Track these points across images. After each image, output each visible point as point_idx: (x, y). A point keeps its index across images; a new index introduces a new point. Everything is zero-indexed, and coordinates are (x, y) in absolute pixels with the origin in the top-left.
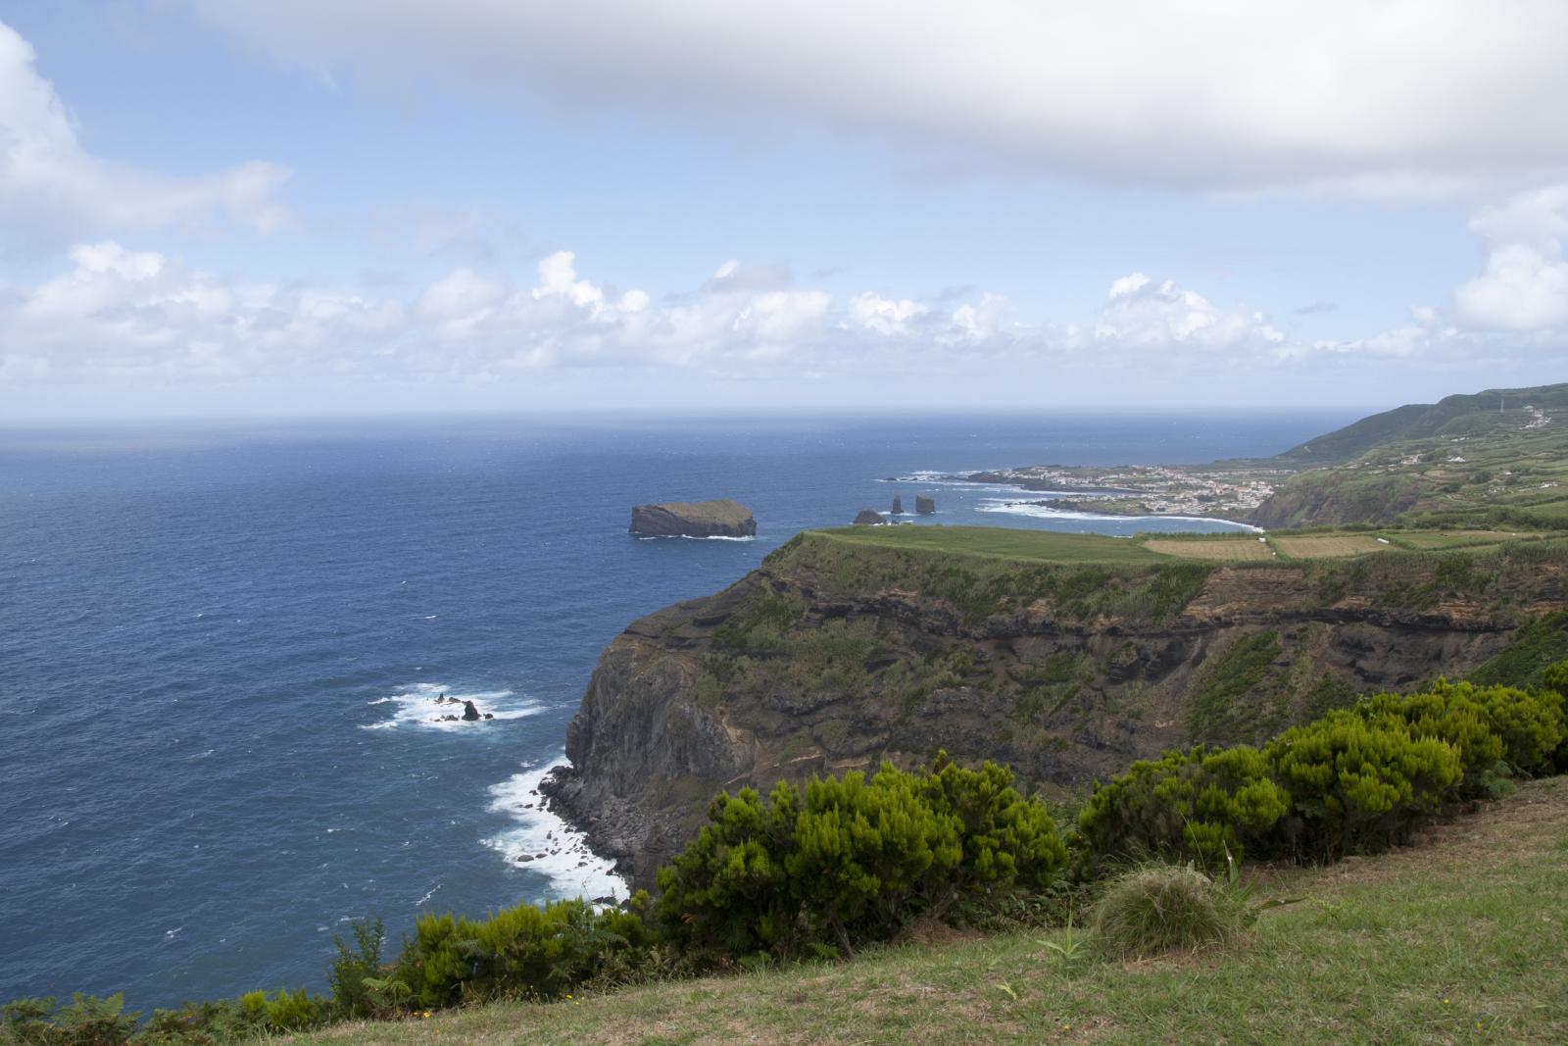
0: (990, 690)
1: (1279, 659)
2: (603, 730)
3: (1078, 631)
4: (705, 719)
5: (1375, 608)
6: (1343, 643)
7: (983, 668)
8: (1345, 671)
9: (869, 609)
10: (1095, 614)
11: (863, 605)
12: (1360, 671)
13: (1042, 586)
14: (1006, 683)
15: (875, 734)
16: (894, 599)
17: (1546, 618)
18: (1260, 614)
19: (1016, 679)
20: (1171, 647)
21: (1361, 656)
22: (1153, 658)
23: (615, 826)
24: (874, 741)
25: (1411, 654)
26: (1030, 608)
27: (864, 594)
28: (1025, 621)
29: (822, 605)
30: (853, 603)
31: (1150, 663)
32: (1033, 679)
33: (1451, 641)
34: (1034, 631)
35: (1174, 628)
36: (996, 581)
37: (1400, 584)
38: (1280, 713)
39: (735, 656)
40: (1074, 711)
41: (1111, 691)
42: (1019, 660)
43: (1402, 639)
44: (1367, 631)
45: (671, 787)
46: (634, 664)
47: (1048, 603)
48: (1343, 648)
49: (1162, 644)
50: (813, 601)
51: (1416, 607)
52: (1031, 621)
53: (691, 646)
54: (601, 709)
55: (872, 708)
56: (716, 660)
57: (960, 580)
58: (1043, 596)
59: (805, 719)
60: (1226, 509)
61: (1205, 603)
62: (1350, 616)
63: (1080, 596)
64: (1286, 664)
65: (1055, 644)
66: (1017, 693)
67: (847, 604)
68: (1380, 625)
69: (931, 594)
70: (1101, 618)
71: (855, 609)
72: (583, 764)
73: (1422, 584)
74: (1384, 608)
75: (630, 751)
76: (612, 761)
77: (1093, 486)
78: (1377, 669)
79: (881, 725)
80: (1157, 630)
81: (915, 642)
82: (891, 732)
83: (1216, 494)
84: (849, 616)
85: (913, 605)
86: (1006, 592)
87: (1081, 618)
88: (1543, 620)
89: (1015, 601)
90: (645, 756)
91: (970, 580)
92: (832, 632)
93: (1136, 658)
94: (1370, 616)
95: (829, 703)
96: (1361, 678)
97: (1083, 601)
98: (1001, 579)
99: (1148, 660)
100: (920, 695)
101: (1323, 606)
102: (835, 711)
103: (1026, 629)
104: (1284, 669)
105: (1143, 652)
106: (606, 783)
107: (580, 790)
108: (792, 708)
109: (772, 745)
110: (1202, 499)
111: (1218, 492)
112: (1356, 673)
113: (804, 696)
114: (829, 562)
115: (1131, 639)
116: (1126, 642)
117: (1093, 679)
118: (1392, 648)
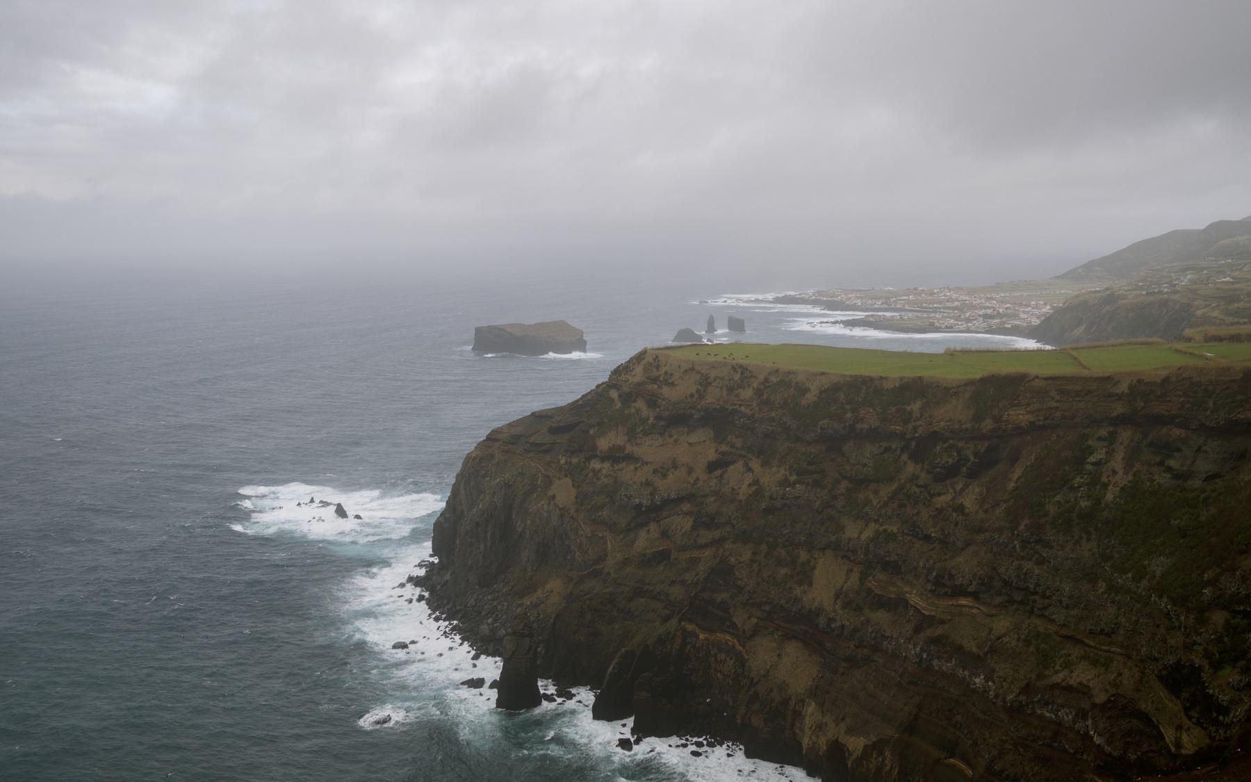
1: (1092, 459)
11: (702, 413)
19: (845, 478)
23: (480, 613)
24: (717, 534)
30: (693, 411)
31: (970, 463)
39: (588, 459)
49: (983, 446)
52: (859, 426)
53: (547, 451)
60: (1009, 326)
65: (880, 446)
71: (695, 417)
77: (886, 306)
78: (1185, 468)
82: (734, 527)
83: (998, 312)
91: (803, 390)
93: (957, 459)
99: (969, 461)
107: (447, 581)
110: (986, 316)
111: (1001, 310)
112: (1164, 472)
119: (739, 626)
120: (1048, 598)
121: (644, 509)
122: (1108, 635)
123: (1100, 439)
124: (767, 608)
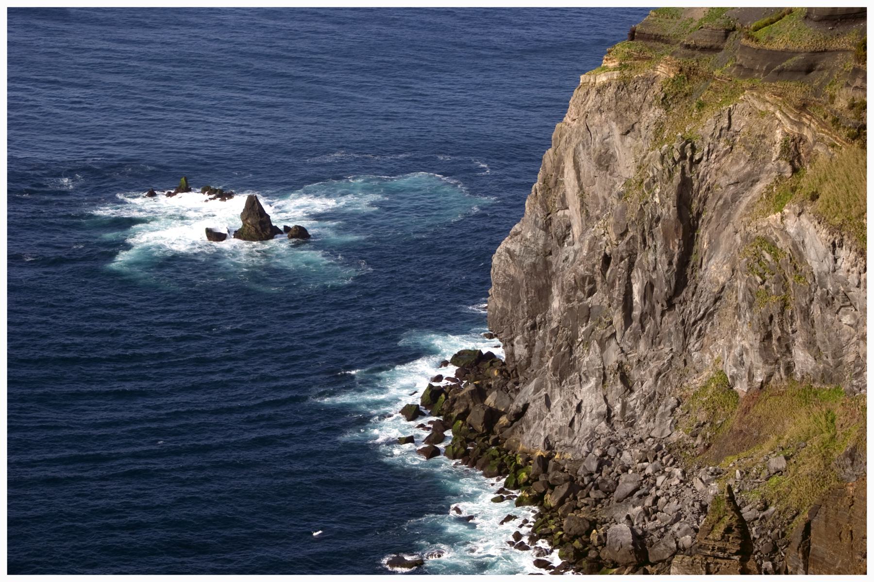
2: (581, 269)
23: (609, 493)
54: (573, 213)
76: (603, 345)
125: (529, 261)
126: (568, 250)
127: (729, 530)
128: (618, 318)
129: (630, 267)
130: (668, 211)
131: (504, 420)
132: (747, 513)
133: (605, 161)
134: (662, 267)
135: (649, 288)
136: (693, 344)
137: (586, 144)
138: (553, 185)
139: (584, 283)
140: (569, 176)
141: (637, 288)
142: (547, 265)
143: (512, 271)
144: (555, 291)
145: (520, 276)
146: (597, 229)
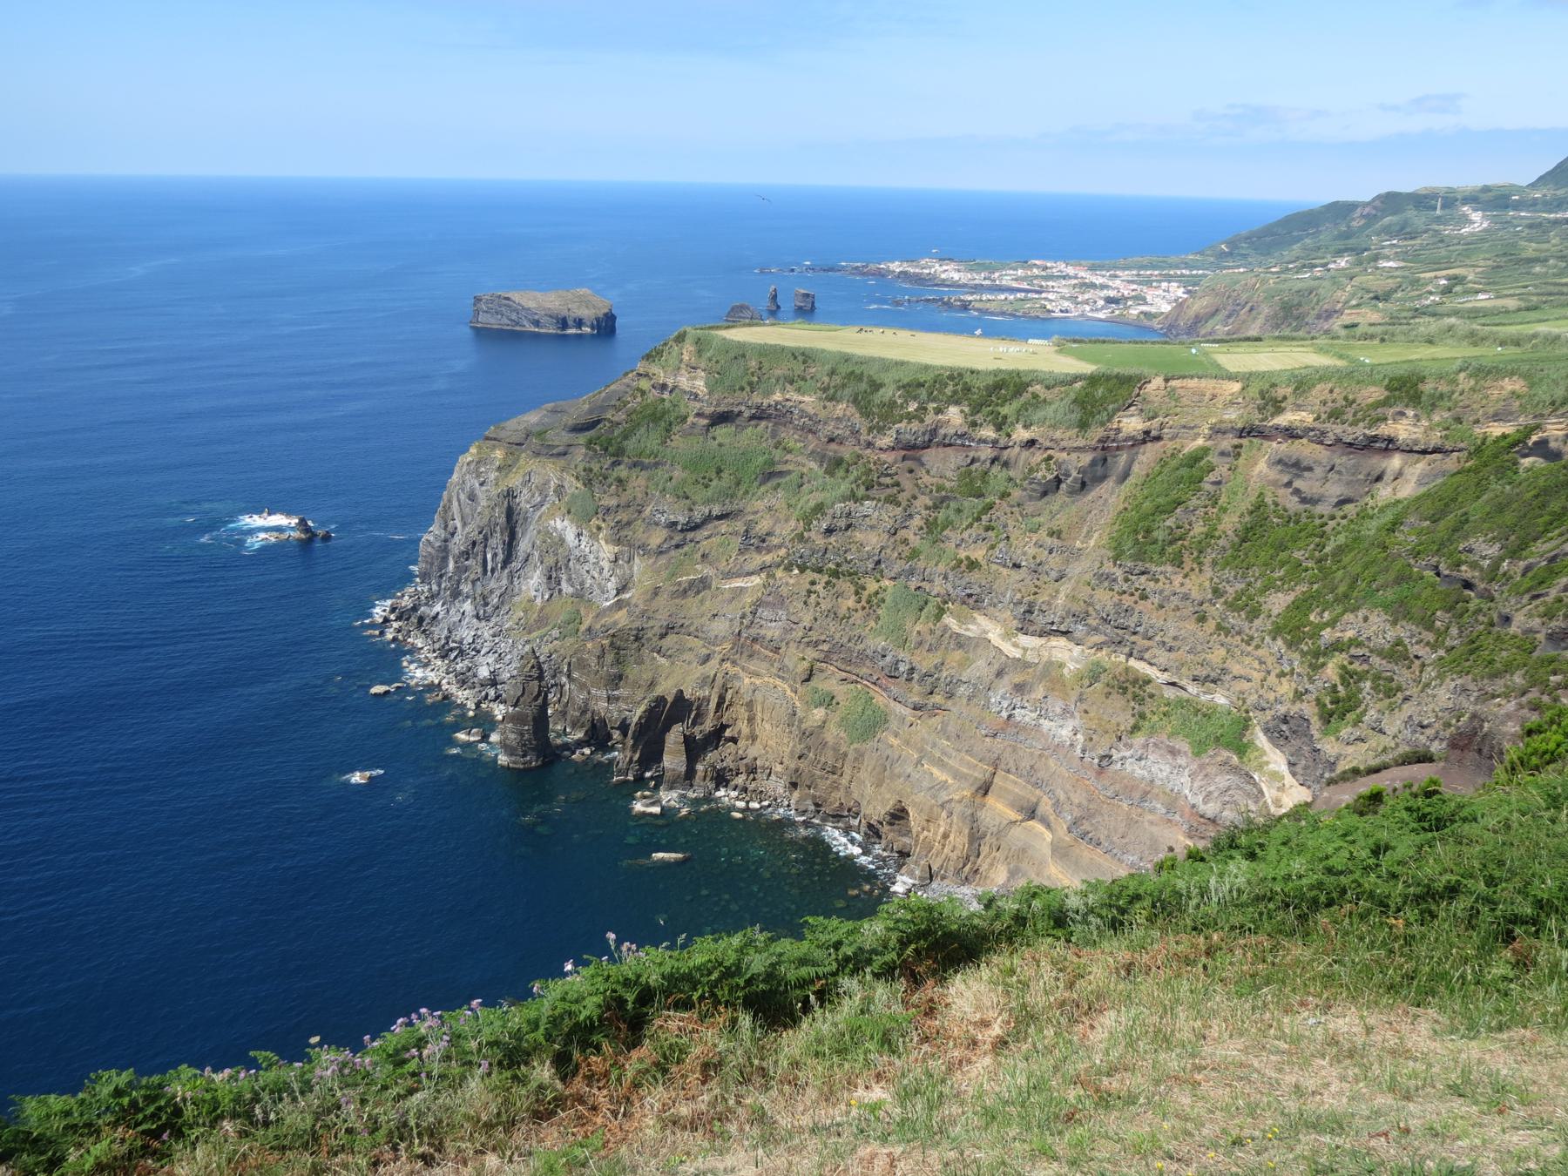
0: (898, 504)
3: (995, 442)
4: (579, 535)
5: (1317, 425)
6: (1280, 462)
7: (888, 480)
8: (1282, 492)
9: (760, 415)
10: (1012, 423)
12: (1297, 492)
13: (955, 392)
14: (915, 498)
15: (769, 551)
16: (789, 404)
17: (1497, 440)
18: (1192, 428)
20: (1093, 463)
21: (1298, 476)
22: (1074, 474)
23: (479, 652)
24: (768, 558)
25: (1353, 474)
26: (940, 417)
27: (757, 399)
28: (934, 432)
29: (709, 410)
30: (743, 408)
32: (943, 493)
33: (1396, 461)
34: (947, 441)
35: (1099, 441)
36: (904, 387)
37: (1346, 399)
38: (1209, 535)
40: (988, 529)
41: (1030, 507)
42: (928, 472)
43: (1344, 458)
44: (1304, 450)
45: (542, 609)
46: (493, 476)
47: (962, 411)
48: (1279, 467)
49: (1086, 459)
50: (698, 405)
51: (1361, 424)
54: (458, 524)
55: (763, 526)
56: (591, 470)
57: (864, 386)
58: (957, 403)
59: (690, 535)
61: (1132, 415)
62: (1290, 433)
63: (997, 405)
64: (1218, 483)
66: (927, 508)
67: (736, 410)
68: (1321, 443)
69: (831, 399)
70: (1019, 426)
72: (439, 585)
73: (1370, 401)
74: (1327, 425)
75: (493, 571)
78: (1314, 491)
79: (775, 541)
80: (1081, 443)
81: (813, 452)
84: (738, 422)
85: (811, 411)
86: (915, 398)
87: (999, 428)
88: (1495, 442)
89: (926, 409)
90: (511, 577)
91: (876, 386)
92: (719, 440)
94: (1311, 434)
95: (719, 518)
96: (1297, 499)
97: (1000, 409)
98: (909, 385)
100: (819, 509)
101: (1263, 420)
102: (724, 526)
103: (932, 439)
104: (1215, 488)
105: (1063, 467)
106: (468, 606)
108: (674, 524)
109: (655, 563)
112: (1292, 494)
113: (691, 510)
114: (717, 362)
115: (1050, 452)
116: (1045, 456)
117: (1009, 494)
118: (1332, 469)
119: (791, 667)
120: (1150, 639)
121: (679, 528)
122: (1214, 682)
123: (1222, 454)
124: (825, 647)
125: (438, 544)
126: (456, 538)
127: (533, 667)
128: (480, 570)
129: (485, 547)
130: (502, 520)
131: (427, 620)
132: (542, 659)
133: (472, 497)
134: (500, 547)
135: (495, 555)
136: (516, 581)
137: (463, 490)
138: (447, 509)
139: (466, 555)
140: (455, 503)
141: (489, 556)
142: (446, 547)
143: (430, 550)
144: (451, 559)
145: (433, 552)
146: (467, 529)
